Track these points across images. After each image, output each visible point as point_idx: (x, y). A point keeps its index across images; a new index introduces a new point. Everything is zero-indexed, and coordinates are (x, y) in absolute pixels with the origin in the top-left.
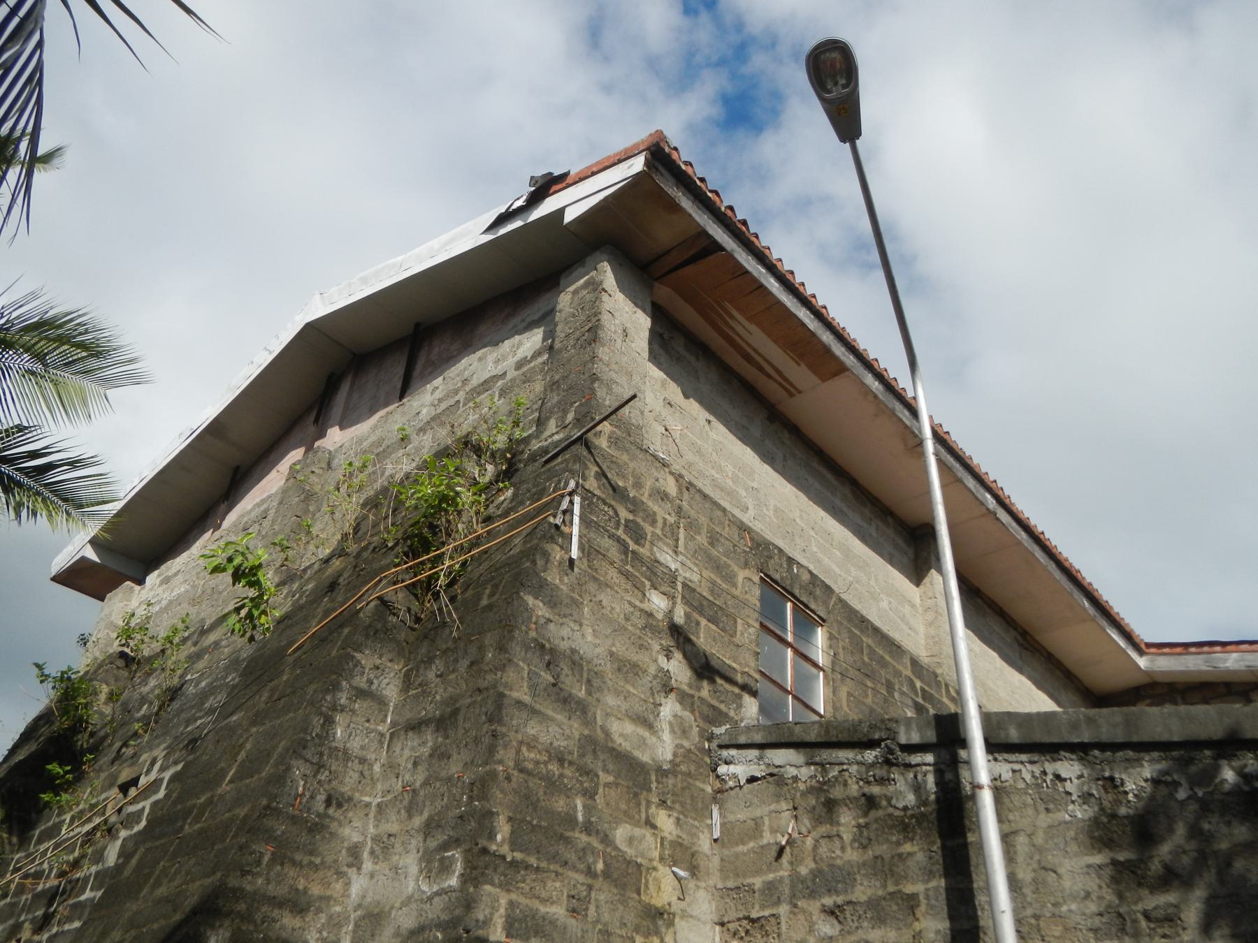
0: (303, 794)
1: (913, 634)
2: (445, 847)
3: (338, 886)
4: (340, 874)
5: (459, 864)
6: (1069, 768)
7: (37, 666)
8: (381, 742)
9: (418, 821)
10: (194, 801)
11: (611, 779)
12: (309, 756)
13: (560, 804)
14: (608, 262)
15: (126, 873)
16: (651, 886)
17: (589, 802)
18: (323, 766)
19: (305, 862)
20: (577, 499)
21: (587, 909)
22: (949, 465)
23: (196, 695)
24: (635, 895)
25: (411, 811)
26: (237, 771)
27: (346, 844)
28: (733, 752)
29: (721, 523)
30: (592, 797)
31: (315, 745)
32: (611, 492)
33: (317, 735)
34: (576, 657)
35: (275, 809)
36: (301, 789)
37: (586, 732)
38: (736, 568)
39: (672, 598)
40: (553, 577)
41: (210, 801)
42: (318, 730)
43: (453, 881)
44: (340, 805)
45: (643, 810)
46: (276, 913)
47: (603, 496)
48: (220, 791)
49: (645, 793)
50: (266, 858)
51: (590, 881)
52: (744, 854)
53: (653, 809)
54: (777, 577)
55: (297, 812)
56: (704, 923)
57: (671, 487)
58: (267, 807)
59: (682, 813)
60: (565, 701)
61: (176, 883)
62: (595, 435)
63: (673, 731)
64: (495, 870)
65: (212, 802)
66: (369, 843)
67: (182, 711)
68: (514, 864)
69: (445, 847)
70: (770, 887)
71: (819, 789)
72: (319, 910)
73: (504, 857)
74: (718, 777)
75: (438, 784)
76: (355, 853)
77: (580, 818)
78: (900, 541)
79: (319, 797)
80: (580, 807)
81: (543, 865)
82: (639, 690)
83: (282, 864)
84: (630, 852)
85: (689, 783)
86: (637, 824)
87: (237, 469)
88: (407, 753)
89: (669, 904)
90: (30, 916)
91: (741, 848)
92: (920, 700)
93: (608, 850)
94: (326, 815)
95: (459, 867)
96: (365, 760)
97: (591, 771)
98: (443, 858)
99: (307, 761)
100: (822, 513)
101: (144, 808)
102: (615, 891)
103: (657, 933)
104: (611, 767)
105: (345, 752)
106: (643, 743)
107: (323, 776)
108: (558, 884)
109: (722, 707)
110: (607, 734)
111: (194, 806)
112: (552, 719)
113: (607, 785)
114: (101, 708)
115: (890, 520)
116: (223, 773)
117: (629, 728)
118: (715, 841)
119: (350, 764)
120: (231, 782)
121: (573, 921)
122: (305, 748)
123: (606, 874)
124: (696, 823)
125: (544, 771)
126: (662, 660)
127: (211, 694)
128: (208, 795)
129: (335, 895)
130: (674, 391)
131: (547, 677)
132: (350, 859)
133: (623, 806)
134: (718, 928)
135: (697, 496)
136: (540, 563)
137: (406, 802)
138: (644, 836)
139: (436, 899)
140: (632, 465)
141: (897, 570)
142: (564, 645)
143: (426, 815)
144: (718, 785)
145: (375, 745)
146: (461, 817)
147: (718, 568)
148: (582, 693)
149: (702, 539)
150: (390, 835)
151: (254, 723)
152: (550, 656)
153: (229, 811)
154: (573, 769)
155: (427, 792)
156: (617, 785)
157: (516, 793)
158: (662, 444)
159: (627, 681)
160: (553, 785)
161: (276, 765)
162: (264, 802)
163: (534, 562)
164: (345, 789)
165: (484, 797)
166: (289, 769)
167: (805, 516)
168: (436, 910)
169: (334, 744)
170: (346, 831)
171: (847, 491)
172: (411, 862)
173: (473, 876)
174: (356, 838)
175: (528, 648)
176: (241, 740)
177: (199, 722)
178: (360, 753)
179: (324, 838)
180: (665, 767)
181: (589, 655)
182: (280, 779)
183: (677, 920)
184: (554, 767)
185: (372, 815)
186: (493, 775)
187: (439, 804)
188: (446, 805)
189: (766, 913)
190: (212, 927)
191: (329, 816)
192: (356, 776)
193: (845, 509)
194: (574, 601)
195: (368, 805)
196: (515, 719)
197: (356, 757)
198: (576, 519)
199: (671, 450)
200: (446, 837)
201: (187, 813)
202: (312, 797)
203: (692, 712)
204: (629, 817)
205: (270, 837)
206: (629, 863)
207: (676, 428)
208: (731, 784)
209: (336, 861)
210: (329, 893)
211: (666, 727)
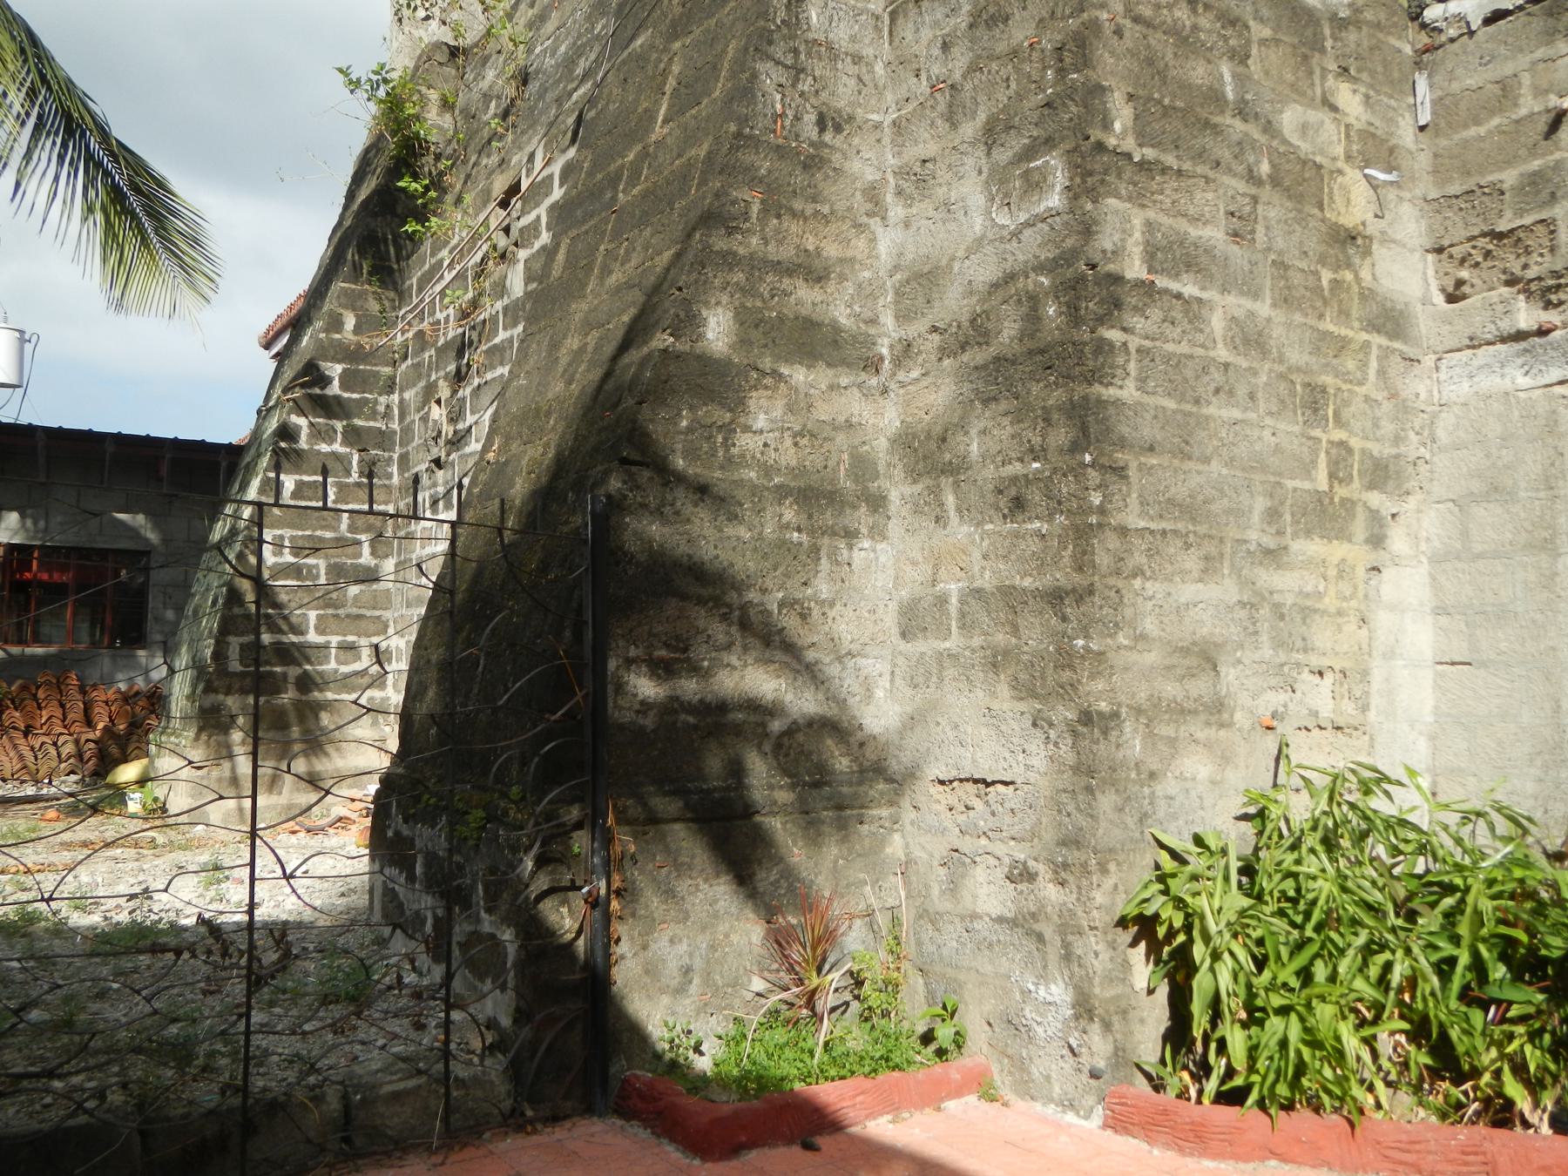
0: (783, 115)
2: (1029, 153)
3: (861, 244)
4: (859, 227)
5: (1059, 174)
7: (340, 70)
8: (877, 29)
9: (970, 129)
10: (620, 162)
11: (1267, 33)
12: (779, 55)
13: (1198, 73)
15: (556, 271)
17: (1240, 69)
18: (803, 70)
19: (808, 212)
21: (1253, 232)
23: (558, 65)
24: (1316, 211)
25: (952, 120)
26: (670, 107)
27: (858, 185)
31: (784, 38)
33: (783, 21)
35: (750, 137)
36: (778, 106)
41: (644, 154)
42: (782, 14)
43: (1055, 200)
44: (838, 129)
45: (1317, 81)
48: (653, 137)
49: (1317, 55)
50: (755, 208)
51: (1253, 191)
52: (1481, 139)
53: (1331, 81)
55: (780, 141)
56: (1412, 251)
58: (739, 135)
59: (1371, 86)
61: (633, 263)
64: (1119, 176)
65: (648, 154)
66: (892, 180)
67: (546, 90)
68: (1145, 166)
69: (1029, 153)
72: (842, 278)
73: (1129, 156)
74: (1424, 26)
75: (994, 66)
76: (873, 194)
77: (1230, 95)
79: (806, 117)
80: (1228, 78)
81: (1187, 166)
83: (779, 216)
84: (1304, 147)
85: (1379, 40)
86: (1311, 103)
88: (926, 34)
89: (1364, 224)
90: (442, 373)
91: (1473, 131)
93: (1275, 143)
94: (822, 145)
95: (1060, 178)
96: (860, 58)
97: (1238, 19)
98: (1027, 172)
99: (778, 63)
101: (538, 217)
102: (1289, 204)
103: (1349, 265)
104: (1265, 12)
107: (806, 85)
108: (1210, 196)
111: (622, 167)
113: (1263, 42)
114: (436, 124)
116: (650, 116)
118: (1422, 128)
119: (840, 66)
120: (666, 121)
121: (1236, 248)
122: (770, 43)
123: (1275, 181)
124: (1393, 102)
125: (1169, 20)
127: (580, 56)
128: (639, 147)
129: (859, 257)
132: (869, 206)
133: (1289, 77)
134: (1430, 257)
137: (942, 107)
138: (1322, 122)
139: (1027, 232)
143: (982, 117)
144: (1424, 39)
145: (869, 34)
146: (1048, 105)
150: (924, 161)
151: (674, 35)
153: (680, 156)
154: (1211, 15)
155: (976, 81)
156: (1277, 41)
157: (1133, 56)
161: (733, 75)
162: (733, 128)
165: (1085, 61)
166: (755, 76)
168: (1032, 246)
169: (811, 36)
172: (971, 191)
174: (870, 175)
176: (662, 66)
177: (575, 96)
178: (853, 48)
179: (827, 177)
180: (1341, 15)
182: (746, 91)
183: (1374, 247)
185: (886, 140)
186: (1094, 26)
187: (1002, 96)
188: (1017, 93)
189: (1528, 220)
190: (707, 304)
191: (826, 145)
192: (852, 82)
195: (878, 126)
197: (847, 54)
200: (1026, 141)
201: (614, 181)
202: (797, 118)
204: (1298, 92)
205: (754, 181)
206: (1305, 162)
208: (1452, 32)
209: (850, 209)
210: (849, 254)
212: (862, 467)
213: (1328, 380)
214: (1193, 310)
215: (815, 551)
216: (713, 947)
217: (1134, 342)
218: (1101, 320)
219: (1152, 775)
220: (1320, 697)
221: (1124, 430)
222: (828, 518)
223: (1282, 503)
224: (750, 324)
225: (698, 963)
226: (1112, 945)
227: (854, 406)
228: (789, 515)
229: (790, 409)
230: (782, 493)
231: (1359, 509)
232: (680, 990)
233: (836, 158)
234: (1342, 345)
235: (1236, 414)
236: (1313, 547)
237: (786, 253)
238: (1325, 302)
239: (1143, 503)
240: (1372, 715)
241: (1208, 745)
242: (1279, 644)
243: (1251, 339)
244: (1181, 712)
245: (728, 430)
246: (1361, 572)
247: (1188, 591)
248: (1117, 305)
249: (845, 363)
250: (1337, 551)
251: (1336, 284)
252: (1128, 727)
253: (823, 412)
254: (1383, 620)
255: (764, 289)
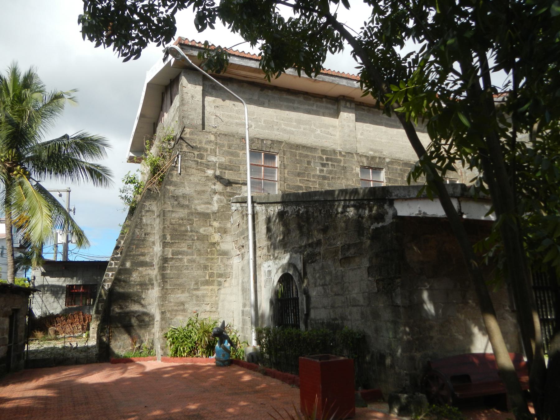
1: (332, 137)
6: (263, 207)
11: (198, 219)
13: (183, 228)
14: (184, 76)
16: (212, 238)
20: (180, 156)
22: (331, 81)
28: (233, 204)
29: (233, 141)
30: (192, 225)
32: (191, 148)
34: (185, 195)
37: (189, 211)
38: (239, 152)
39: (215, 170)
40: (174, 179)
44: (148, 235)
46: (139, 257)
47: (189, 151)
50: (134, 248)
53: (212, 222)
54: (256, 148)
57: (212, 138)
58: (132, 239)
60: (182, 206)
62: (185, 135)
63: (217, 202)
68: (172, 243)
70: (238, 233)
71: (242, 213)
72: (148, 255)
77: (189, 230)
78: (330, 106)
81: (180, 241)
82: (205, 197)
84: (204, 233)
86: (207, 227)
87: (154, 124)
92: (325, 162)
100: (287, 112)
103: (214, 247)
104: (197, 216)
105: (147, 224)
106: (208, 208)
107: (143, 230)
109: (235, 192)
110: (196, 209)
112: (179, 211)
115: (324, 100)
117: (203, 206)
123: (198, 239)
126: (213, 187)
130: (219, 101)
131: (176, 203)
135: (223, 136)
136: (170, 177)
140: (198, 138)
141: (327, 117)
142: (181, 194)
145: (153, 221)
147: (232, 154)
148: (187, 203)
149: (226, 148)
152: (176, 198)
156: (199, 220)
158: (215, 121)
159: (201, 195)
160: (180, 225)
163: (168, 178)
164: (148, 231)
166: (134, 231)
167: (278, 117)
170: (151, 239)
171: (301, 99)
173: (164, 247)
174: (153, 240)
175: (169, 198)
181: (189, 193)
184: (181, 222)
193: (299, 106)
194: (183, 183)
195: (154, 233)
196: (169, 215)
198: (180, 163)
199: (218, 121)
203: (224, 196)
204: (203, 226)
205: (134, 244)
207: (219, 113)
211: (215, 202)
212: (150, 280)
213: (209, 264)
214: (181, 260)
215: (142, 292)
216: (124, 343)
217: (169, 266)
218: (164, 264)
219: (171, 319)
220: (208, 308)
221: (168, 277)
222: (145, 287)
223: (198, 282)
224: (133, 264)
225: (122, 345)
226: (164, 340)
227: (150, 272)
228: (138, 287)
229: (139, 273)
230: (137, 285)
231: (216, 281)
232: (120, 348)
233: (147, 239)
234: (212, 259)
235: (189, 271)
236: (206, 287)
237: (139, 253)
238: (208, 253)
239: (170, 285)
240: (219, 310)
241: (182, 315)
242: (197, 301)
243: (193, 261)
244: (177, 311)
245: (129, 277)
246: (216, 290)
247: (179, 295)
248: (167, 261)
249: (148, 266)
250: (211, 287)
251: (211, 251)
252: (167, 313)
253: (144, 273)
254: (222, 297)
255: (135, 258)
